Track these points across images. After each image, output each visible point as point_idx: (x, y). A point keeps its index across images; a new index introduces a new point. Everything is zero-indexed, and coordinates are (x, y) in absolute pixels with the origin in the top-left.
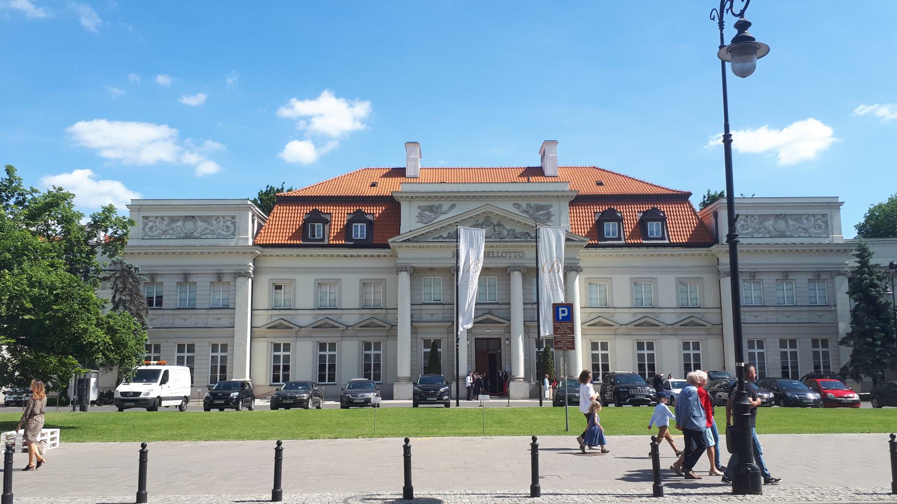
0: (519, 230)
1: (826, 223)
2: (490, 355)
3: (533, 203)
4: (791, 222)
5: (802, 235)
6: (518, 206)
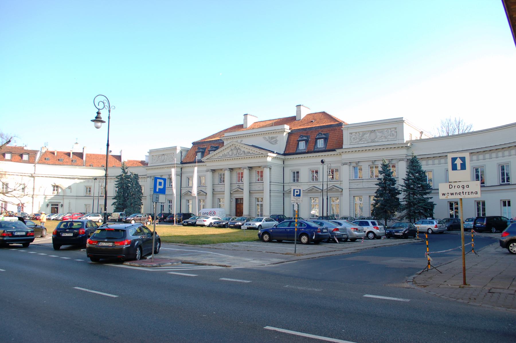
0: (246, 151)
1: (396, 132)
2: (503, 202)
3: (271, 136)
4: (378, 134)
5: (384, 140)
6: (265, 138)
